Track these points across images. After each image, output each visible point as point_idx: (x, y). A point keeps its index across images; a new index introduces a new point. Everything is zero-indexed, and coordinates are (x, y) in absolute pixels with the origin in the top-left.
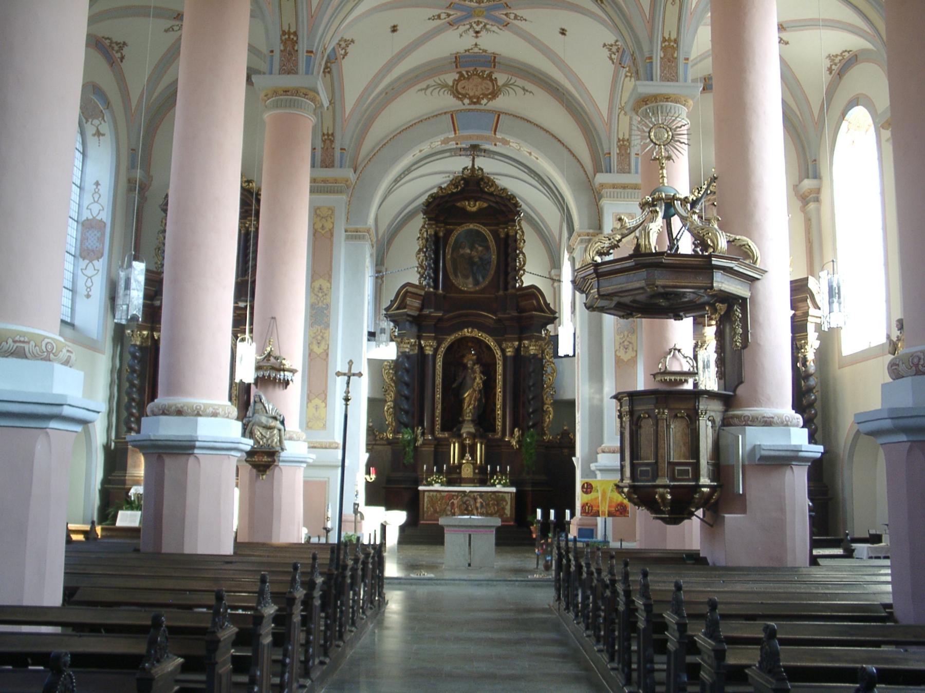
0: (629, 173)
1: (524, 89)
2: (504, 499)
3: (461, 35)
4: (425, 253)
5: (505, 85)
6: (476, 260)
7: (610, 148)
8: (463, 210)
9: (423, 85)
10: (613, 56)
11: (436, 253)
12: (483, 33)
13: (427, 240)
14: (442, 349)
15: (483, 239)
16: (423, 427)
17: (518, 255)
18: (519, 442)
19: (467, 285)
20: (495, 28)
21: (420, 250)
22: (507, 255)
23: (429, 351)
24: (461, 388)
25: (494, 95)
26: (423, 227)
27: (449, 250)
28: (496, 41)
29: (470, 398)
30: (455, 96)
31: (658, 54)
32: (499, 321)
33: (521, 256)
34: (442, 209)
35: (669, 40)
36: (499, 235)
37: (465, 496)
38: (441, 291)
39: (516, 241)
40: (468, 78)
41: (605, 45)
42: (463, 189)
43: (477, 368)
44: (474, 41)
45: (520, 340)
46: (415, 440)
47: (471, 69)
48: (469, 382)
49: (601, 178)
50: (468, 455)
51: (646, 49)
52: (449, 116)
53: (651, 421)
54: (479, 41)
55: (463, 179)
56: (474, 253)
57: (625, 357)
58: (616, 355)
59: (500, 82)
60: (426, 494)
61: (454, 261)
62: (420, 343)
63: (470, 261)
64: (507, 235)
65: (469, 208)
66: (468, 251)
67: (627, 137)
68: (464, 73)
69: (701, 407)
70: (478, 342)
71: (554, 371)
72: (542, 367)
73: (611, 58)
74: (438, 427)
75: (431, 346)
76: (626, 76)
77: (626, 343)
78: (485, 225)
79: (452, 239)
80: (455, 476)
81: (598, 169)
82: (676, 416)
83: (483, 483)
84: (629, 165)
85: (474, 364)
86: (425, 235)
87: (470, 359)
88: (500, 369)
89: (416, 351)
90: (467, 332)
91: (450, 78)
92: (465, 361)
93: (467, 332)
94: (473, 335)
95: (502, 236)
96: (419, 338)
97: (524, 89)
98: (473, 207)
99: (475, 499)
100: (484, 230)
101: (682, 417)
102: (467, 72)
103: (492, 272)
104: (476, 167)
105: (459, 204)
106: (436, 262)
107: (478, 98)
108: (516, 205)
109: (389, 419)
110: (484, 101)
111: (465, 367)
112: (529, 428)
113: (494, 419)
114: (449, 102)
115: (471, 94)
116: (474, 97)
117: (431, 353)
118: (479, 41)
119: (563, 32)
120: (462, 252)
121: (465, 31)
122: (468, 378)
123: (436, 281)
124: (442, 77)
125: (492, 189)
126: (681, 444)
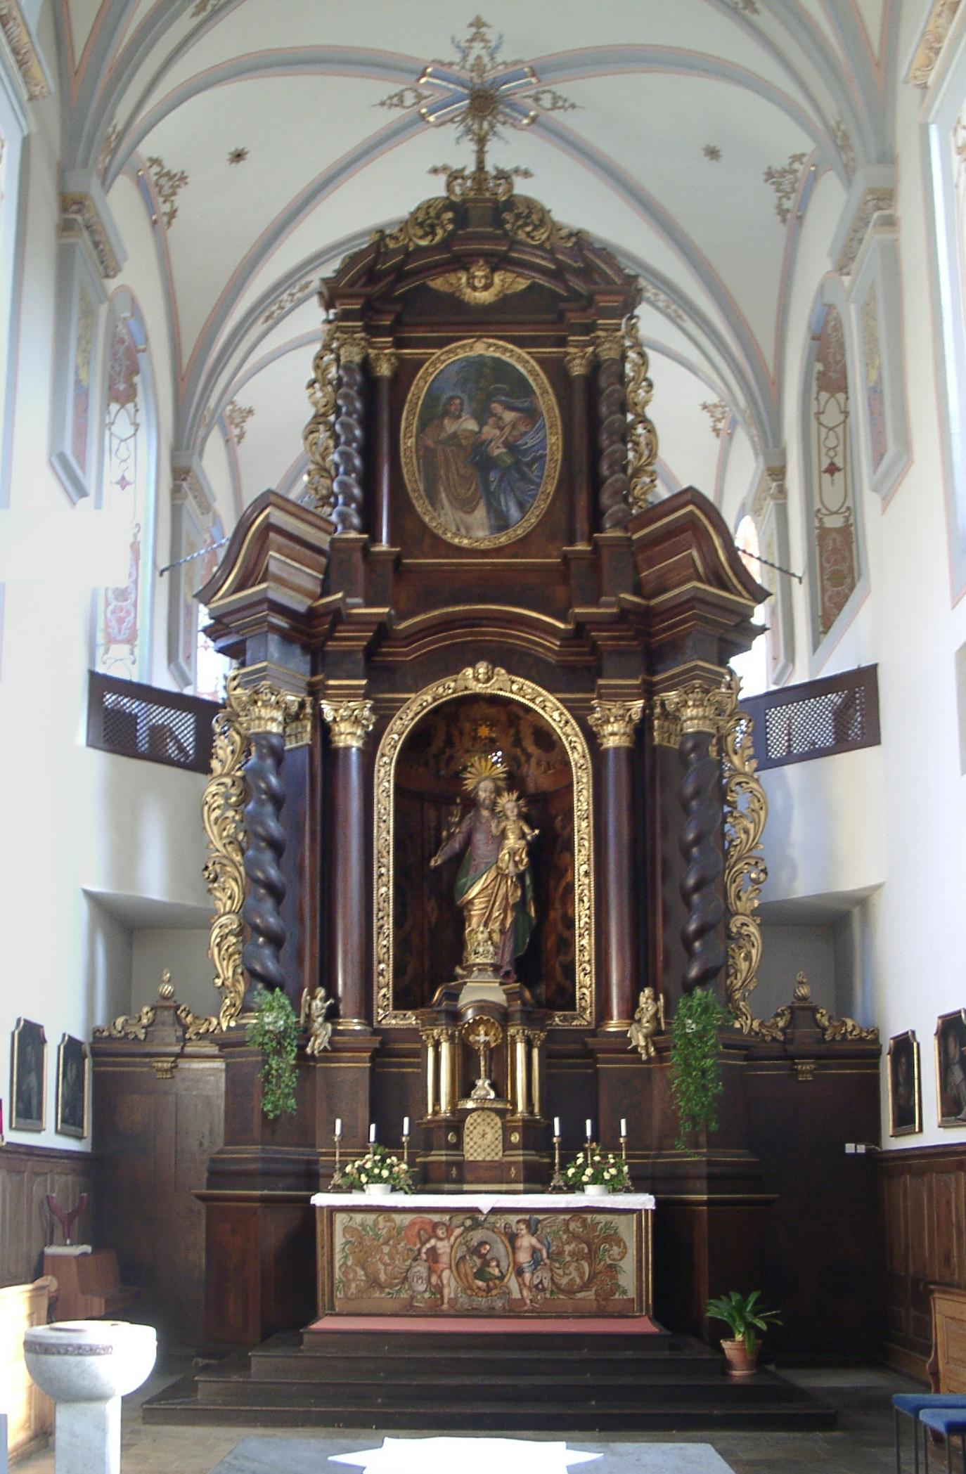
2: (613, 1238)
6: (498, 451)
11: (369, 421)
15: (521, 387)
16: (331, 993)
18: (655, 1034)
19: (468, 529)
21: (319, 419)
23: (349, 738)
24: (459, 863)
26: (327, 347)
27: (409, 421)
32: (581, 630)
34: (385, 292)
37: (477, 1225)
38: (384, 546)
46: (306, 1034)
50: (483, 1084)
55: (449, 205)
56: (489, 431)
60: (340, 1218)
61: (427, 457)
62: (318, 714)
63: (481, 460)
66: (472, 425)
71: (762, 802)
72: (722, 793)
74: (384, 993)
75: (357, 721)
78: (520, 342)
79: (419, 389)
80: (439, 1156)
83: (538, 1179)
86: (333, 373)
87: (485, 773)
88: (582, 801)
89: (307, 739)
93: (476, 679)
96: (315, 692)
98: (481, 288)
99: (512, 1238)
100: (521, 360)
103: (551, 489)
104: (489, 168)
105: (438, 284)
109: (227, 971)
112: (688, 988)
117: (355, 744)
120: (450, 426)
125: (541, 235)
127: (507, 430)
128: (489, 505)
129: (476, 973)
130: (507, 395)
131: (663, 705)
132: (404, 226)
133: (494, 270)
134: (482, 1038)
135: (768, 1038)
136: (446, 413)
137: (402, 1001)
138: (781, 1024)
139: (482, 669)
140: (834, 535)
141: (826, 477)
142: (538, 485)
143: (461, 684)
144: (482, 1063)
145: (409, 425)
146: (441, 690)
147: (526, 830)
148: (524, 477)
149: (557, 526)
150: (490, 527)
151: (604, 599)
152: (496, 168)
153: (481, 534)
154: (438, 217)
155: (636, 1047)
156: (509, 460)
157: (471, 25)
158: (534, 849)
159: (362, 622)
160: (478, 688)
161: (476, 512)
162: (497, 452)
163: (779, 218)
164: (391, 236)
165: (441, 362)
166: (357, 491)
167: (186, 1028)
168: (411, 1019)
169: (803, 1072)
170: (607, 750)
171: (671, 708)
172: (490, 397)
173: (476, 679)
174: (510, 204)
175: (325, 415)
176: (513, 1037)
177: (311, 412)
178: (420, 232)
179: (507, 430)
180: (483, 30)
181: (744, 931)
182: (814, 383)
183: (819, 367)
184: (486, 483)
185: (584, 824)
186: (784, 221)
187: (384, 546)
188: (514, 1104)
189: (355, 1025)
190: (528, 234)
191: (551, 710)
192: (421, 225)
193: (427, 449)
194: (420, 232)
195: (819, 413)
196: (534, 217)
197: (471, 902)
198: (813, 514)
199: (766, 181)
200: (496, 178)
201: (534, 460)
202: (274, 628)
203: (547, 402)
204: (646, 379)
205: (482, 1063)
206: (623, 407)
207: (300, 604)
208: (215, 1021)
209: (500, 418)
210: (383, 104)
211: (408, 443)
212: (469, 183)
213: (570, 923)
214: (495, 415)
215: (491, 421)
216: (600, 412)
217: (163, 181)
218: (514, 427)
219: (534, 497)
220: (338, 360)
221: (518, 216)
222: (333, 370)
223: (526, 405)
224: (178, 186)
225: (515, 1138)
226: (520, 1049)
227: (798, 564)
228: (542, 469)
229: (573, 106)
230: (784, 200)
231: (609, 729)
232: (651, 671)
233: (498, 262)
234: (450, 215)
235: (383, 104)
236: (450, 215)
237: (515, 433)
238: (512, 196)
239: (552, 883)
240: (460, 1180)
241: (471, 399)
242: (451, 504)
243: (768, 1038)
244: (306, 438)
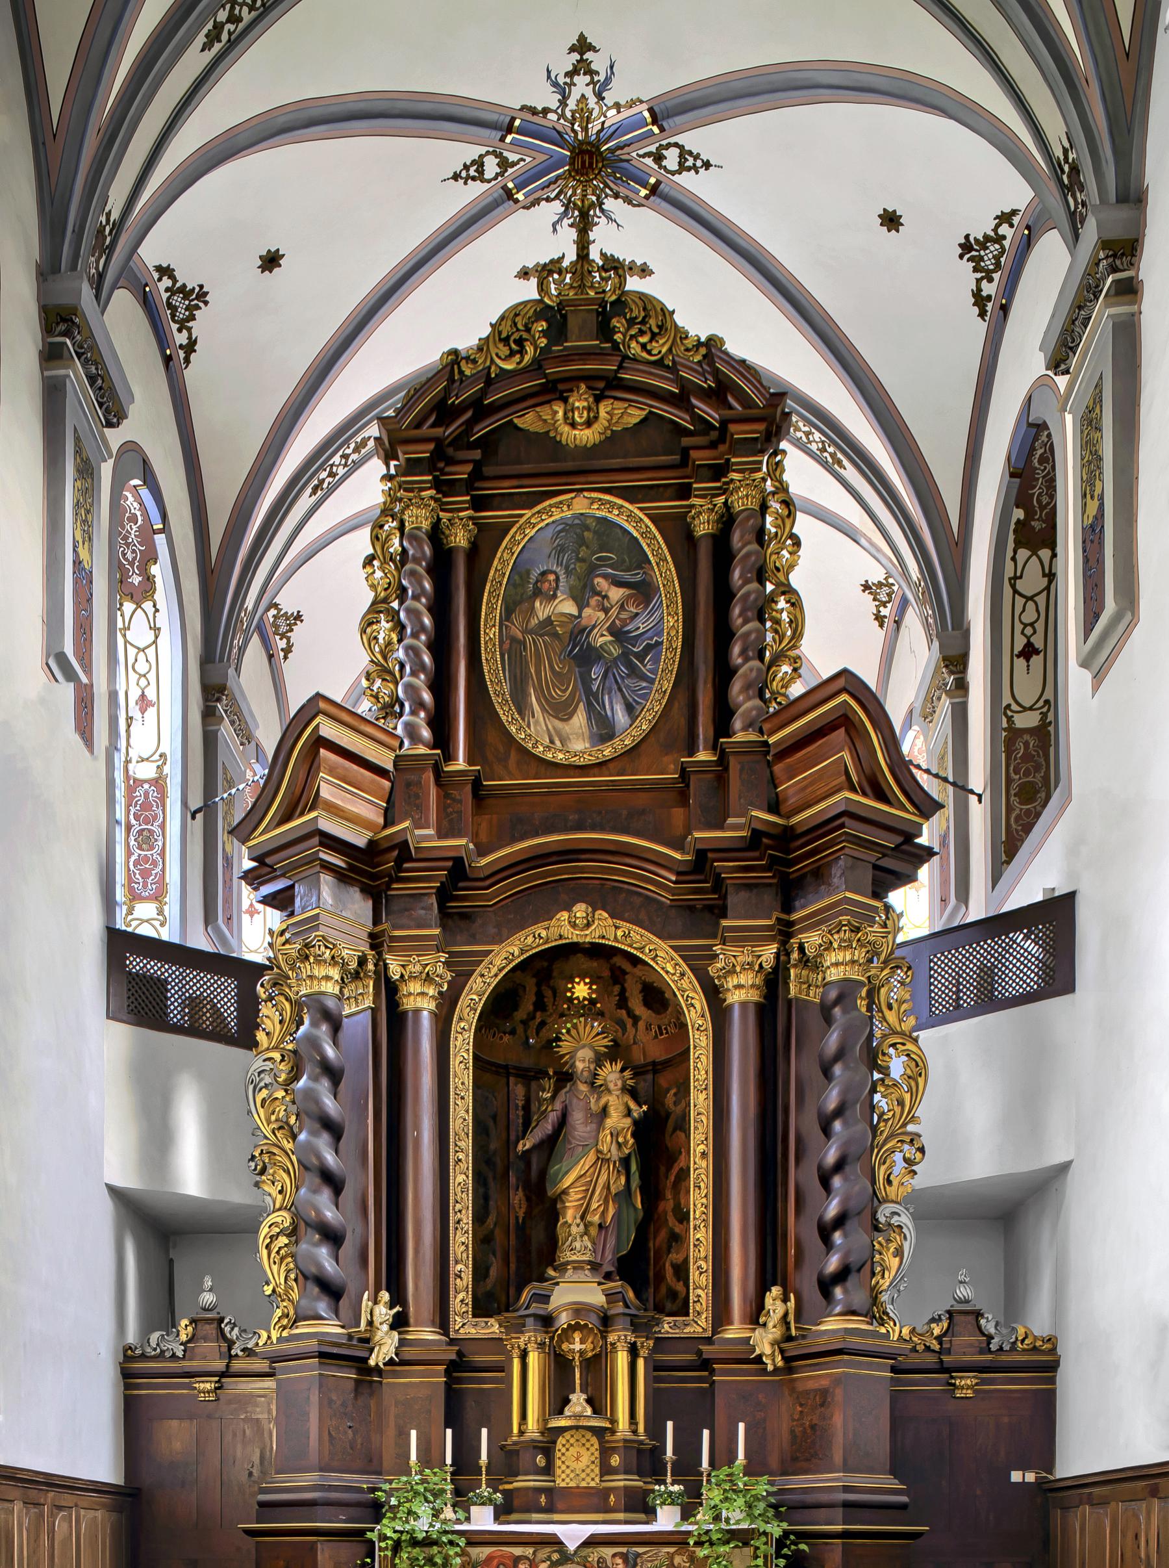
6: (601, 639)
8: (548, 443)
19: (567, 739)
21: (378, 606)
29: (588, 1187)
34: (458, 435)
38: (460, 763)
43: (611, 1074)
48: (579, 1125)
50: (578, 1402)
55: (541, 311)
56: (591, 614)
61: (514, 651)
65: (568, 435)
66: (569, 608)
70: (609, 963)
78: (630, 494)
80: (525, 1482)
85: (599, 1060)
89: (368, 1002)
94: (590, 936)
95: (703, 526)
100: (632, 519)
103: (668, 686)
104: (594, 254)
105: (528, 421)
120: (542, 610)
122: (577, 1117)
125: (660, 347)
128: (590, 708)
129: (570, 1272)
130: (611, 567)
131: (801, 948)
132: (483, 346)
133: (598, 399)
134: (577, 1346)
136: (537, 592)
137: (482, 1307)
138: (937, 1331)
139: (580, 910)
142: (652, 682)
143: (554, 932)
144: (577, 1375)
145: (491, 610)
146: (530, 939)
147: (632, 1105)
148: (634, 672)
149: (674, 731)
150: (592, 736)
151: (730, 820)
152: (603, 255)
153: (579, 745)
155: (760, 1357)
156: (615, 651)
157: (572, 49)
158: (641, 1129)
159: (431, 858)
160: (574, 936)
161: (575, 718)
162: (601, 640)
163: (976, 310)
164: (467, 359)
165: (536, 527)
166: (427, 696)
167: (231, 1344)
168: (493, 1327)
169: (962, 1388)
171: (810, 952)
172: (592, 570)
173: (574, 924)
174: (620, 304)
175: (385, 600)
178: (505, 351)
179: (614, 612)
180: (589, 55)
181: (895, 1220)
184: (586, 681)
185: (702, 1096)
186: (982, 314)
187: (460, 763)
188: (613, 1421)
189: (427, 1334)
190: (644, 346)
191: (665, 960)
192: (506, 341)
193: (513, 640)
194: (505, 351)
196: (652, 322)
197: (565, 1192)
199: (961, 257)
200: (603, 268)
201: (649, 648)
202: (327, 867)
203: (664, 572)
205: (577, 1375)
206: (761, 576)
207: (359, 839)
208: (264, 1335)
209: (606, 597)
210: (456, 177)
211: (489, 633)
213: (683, 1217)
214: (598, 594)
215: (594, 601)
216: (730, 583)
217: (177, 300)
218: (622, 607)
219: (645, 697)
223: (638, 578)
224: (198, 308)
225: (615, 1460)
228: (656, 660)
229: (707, 165)
230: (984, 283)
231: (732, 982)
232: (788, 908)
233: (607, 386)
234: (542, 325)
235: (456, 177)
236: (542, 325)
237: (624, 616)
238: (624, 293)
239: (663, 1169)
241: (568, 573)
242: (543, 709)
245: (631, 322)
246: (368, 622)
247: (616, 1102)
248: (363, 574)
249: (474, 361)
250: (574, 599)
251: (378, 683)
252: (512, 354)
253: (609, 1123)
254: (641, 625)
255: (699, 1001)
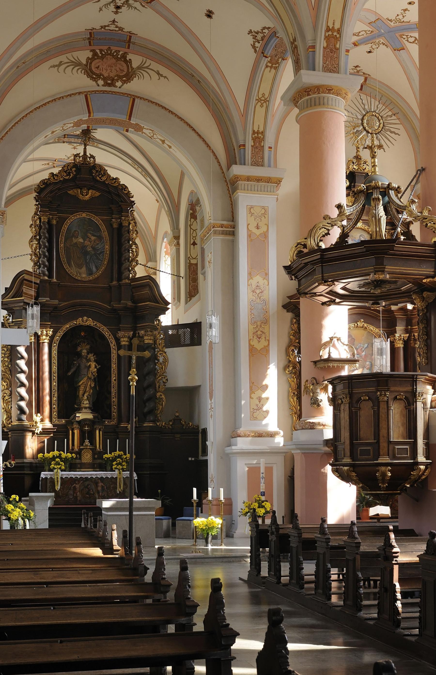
0: (262, 166)
1: (158, 73)
3: (101, 9)
4: (39, 240)
5: (139, 68)
6: (89, 249)
7: (245, 140)
8: (75, 198)
9: (56, 61)
10: (257, 45)
11: (50, 241)
12: (124, 9)
13: (40, 227)
14: (57, 338)
17: (131, 246)
20: (137, 5)
22: (120, 245)
25: (128, 77)
26: (36, 214)
27: (62, 238)
28: (136, 21)
30: (89, 76)
31: (321, 44)
33: (134, 247)
35: (333, 30)
36: (111, 225)
39: (129, 232)
40: (102, 58)
41: (250, 32)
42: (75, 177)
43: (91, 357)
44: (113, 16)
45: (135, 329)
47: (105, 48)
49: (237, 170)
51: (309, 36)
52: (83, 97)
53: (370, 404)
54: (117, 17)
55: (75, 165)
56: (87, 243)
57: (258, 346)
58: (250, 345)
59: (135, 65)
64: (121, 225)
65: (81, 197)
66: (81, 240)
67: (261, 129)
68: (98, 51)
69: (418, 390)
73: (254, 47)
76: (267, 66)
77: (259, 333)
79: (65, 227)
81: (232, 160)
82: (395, 398)
84: (263, 158)
86: (38, 222)
90: (79, 321)
91: (84, 56)
92: (79, 349)
95: (115, 226)
97: (158, 73)
100: (97, 219)
101: (400, 399)
102: (101, 51)
104: (88, 154)
105: (70, 192)
106: (50, 250)
107: (113, 80)
108: (129, 195)
110: (119, 84)
111: (79, 355)
113: (110, 406)
114: (83, 82)
115: (106, 75)
116: (109, 78)
118: (117, 17)
119: (209, 14)
120: (75, 240)
121: (106, 5)
123: (50, 269)
124: (75, 54)
125: (104, 178)
126: (400, 424)
127: (92, 242)
128: (87, 266)
130: (92, 231)
133: (89, 190)
135: (167, 428)
140: (194, 266)
141: (192, 246)
142: (102, 261)
143: (78, 323)
146: (72, 324)
152: (90, 154)
153: (84, 276)
154: (71, 170)
156: (93, 253)
160: (82, 323)
161: (83, 269)
164: (56, 175)
165: (73, 220)
170: (122, 345)
176: (95, 428)
177: (31, 235)
179: (92, 242)
182: (189, 216)
183: (191, 212)
191: (105, 331)
192: (66, 172)
194: (65, 174)
195: (190, 225)
198: (187, 258)
200: (90, 158)
201: (101, 253)
203: (105, 234)
204: (136, 231)
209: (90, 239)
212: (81, 159)
220: (40, 219)
221: (97, 171)
222: (38, 222)
223: (99, 235)
226: (97, 432)
227: (182, 274)
234: (74, 169)
236: (74, 169)
238: (95, 164)
240: (80, 468)
243: (167, 428)
244: (30, 244)
245: (97, 171)
246: (31, 241)
247: (93, 364)
248: (30, 229)
249: (57, 176)
250: (82, 238)
251: (34, 257)
252: (67, 175)
253: (91, 369)
254: (99, 246)
255: (114, 342)
